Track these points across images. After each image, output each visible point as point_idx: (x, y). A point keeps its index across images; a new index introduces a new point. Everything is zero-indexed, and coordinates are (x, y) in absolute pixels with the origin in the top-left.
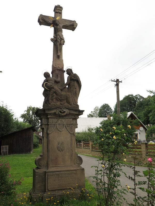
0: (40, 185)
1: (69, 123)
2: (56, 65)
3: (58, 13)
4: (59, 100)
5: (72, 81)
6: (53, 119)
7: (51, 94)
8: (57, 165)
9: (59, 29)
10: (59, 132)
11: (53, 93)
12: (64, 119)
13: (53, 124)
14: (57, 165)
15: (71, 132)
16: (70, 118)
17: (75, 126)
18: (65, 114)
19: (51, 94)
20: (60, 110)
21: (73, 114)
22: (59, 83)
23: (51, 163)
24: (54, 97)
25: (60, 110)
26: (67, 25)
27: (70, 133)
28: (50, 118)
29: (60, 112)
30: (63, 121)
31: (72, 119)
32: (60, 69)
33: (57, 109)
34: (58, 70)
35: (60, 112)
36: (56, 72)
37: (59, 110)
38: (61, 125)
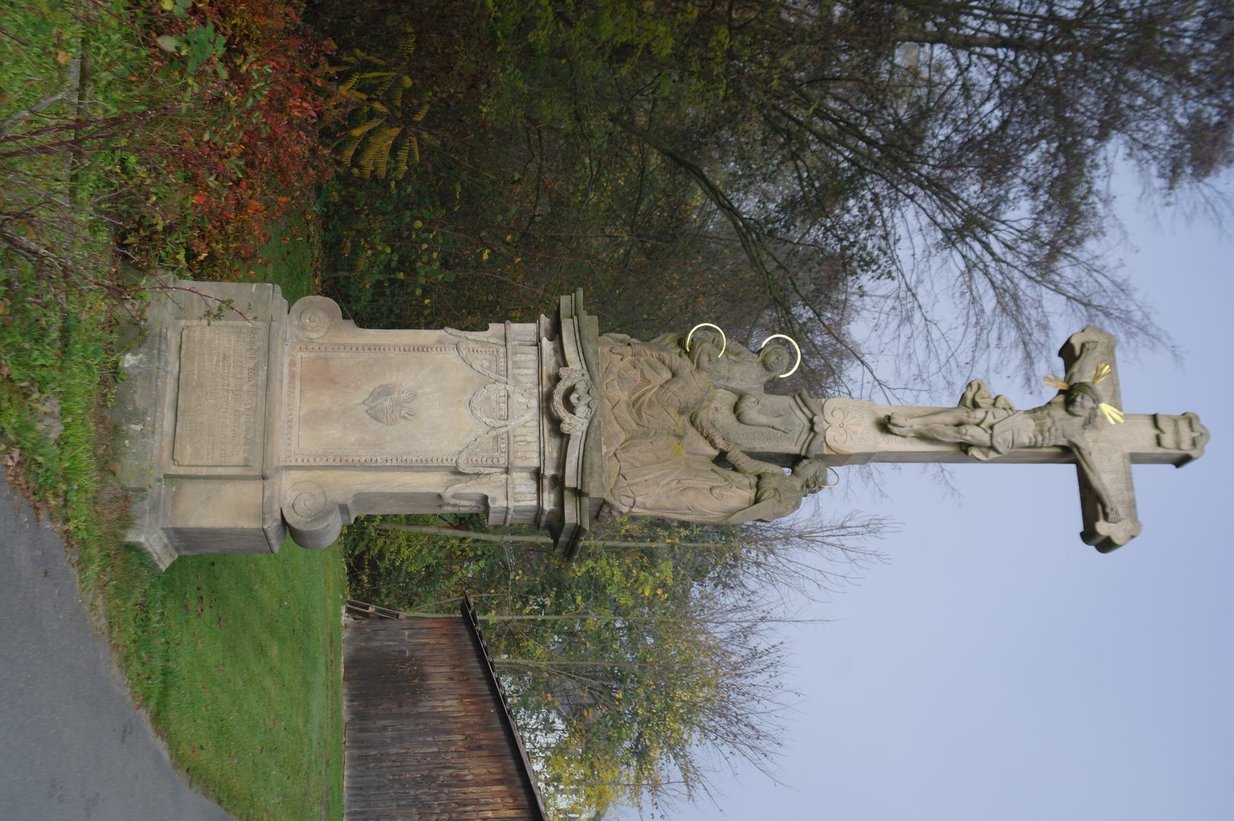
1: (513, 447)
2: (838, 414)
3: (1157, 432)
4: (637, 394)
5: (754, 480)
6: (534, 365)
7: (665, 355)
8: (298, 383)
9: (1049, 414)
10: (466, 398)
12: (536, 423)
13: (510, 366)
15: (465, 454)
16: (541, 453)
17: (503, 491)
18: (561, 412)
19: (665, 355)
20: (578, 386)
21: (561, 465)
22: (733, 418)
23: (313, 355)
24: (649, 374)
25: (581, 387)
26: (1092, 471)
29: (572, 389)
30: (528, 417)
31: (535, 463)
32: (816, 429)
33: (585, 371)
34: (811, 421)
35: (572, 389)
36: (798, 412)
37: (583, 383)
38: (504, 406)
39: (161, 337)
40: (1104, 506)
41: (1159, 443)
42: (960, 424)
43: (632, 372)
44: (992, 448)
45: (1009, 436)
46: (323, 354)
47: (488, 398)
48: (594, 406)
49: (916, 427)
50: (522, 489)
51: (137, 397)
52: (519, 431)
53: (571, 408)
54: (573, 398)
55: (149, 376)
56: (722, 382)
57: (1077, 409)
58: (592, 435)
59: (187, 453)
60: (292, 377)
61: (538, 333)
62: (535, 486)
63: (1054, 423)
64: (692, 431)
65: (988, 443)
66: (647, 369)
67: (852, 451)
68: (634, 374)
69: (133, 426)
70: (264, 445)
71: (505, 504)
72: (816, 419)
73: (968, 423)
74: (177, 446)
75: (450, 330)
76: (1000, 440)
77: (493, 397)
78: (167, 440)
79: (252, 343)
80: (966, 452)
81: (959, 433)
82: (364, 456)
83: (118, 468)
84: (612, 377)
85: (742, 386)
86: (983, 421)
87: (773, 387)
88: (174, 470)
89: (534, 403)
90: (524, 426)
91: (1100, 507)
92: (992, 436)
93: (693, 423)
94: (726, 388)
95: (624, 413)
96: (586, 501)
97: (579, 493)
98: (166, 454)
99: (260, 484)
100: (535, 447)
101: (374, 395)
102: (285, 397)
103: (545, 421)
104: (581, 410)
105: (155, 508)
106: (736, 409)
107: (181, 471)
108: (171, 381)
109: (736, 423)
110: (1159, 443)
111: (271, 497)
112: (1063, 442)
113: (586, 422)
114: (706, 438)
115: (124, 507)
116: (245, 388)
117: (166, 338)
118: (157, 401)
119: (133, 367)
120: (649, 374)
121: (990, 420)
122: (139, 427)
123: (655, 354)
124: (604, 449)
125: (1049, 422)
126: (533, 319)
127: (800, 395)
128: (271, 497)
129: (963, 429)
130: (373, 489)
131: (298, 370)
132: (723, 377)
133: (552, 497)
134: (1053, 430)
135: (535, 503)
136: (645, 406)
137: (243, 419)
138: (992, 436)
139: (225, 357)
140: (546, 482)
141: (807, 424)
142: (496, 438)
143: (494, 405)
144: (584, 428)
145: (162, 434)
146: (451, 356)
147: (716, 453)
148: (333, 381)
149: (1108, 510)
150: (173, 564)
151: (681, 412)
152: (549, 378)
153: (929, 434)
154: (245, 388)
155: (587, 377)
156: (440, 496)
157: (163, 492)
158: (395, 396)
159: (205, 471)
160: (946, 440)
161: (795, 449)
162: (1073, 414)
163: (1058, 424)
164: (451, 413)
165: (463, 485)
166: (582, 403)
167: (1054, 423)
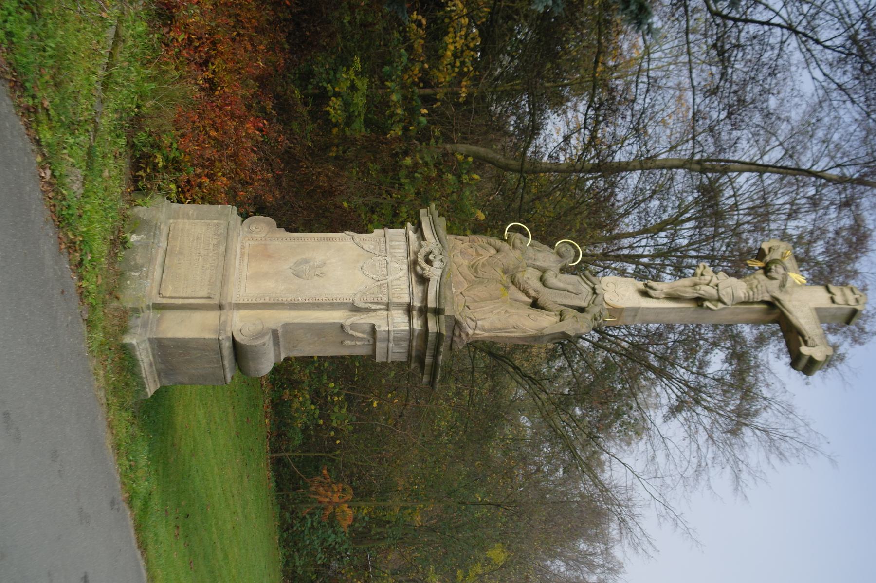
3: (830, 295)
8: (246, 259)
11: (495, 248)
12: (406, 278)
14: (246, 259)
16: (411, 294)
17: (385, 321)
21: (425, 298)
24: (481, 251)
25: (436, 252)
26: (791, 313)
29: (430, 252)
31: (406, 299)
32: (597, 292)
34: (594, 289)
39: (157, 227)
40: (803, 337)
41: (833, 301)
42: (696, 284)
43: (470, 250)
44: (720, 300)
45: (729, 290)
49: (665, 290)
50: (399, 320)
51: (138, 258)
52: (395, 283)
53: (429, 262)
54: (431, 257)
55: (146, 246)
56: (530, 261)
57: (773, 274)
58: (445, 276)
59: (169, 291)
60: (243, 255)
62: (407, 319)
63: (759, 282)
64: (512, 287)
65: (716, 296)
66: (479, 249)
67: (623, 306)
68: (472, 251)
69: (133, 273)
70: (222, 287)
71: (387, 329)
72: (596, 286)
73: (700, 284)
74: (163, 286)
75: (347, 232)
76: (724, 293)
77: (377, 264)
78: (156, 284)
79: (216, 231)
80: (702, 306)
81: (696, 289)
82: (290, 298)
83: (121, 297)
84: (456, 251)
85: (544, 265)
86: (710, 282)
87: (564, 270)
88: (159, 300)
89: (405, 267)
90: (398, 279)
91: (800, 338)
92: (718, 290)
93: (513, 282)
94: (534, 267)
96: (442, 317)
97: (438, 312)
99: (218, 313)
101: (297, 264)
102: (237, 265)
103: (413, 276)
104: (437, 264)
105: (145, 325)
106: (542, 279)
107: (164, 301)
108: (161, 252)
109: (542, 287)
110: (833, 301)
111: (225, 322)
112: (767, 298)
113: (440, 271)
114: (522, 291)
115: (123, 321)
116: (210, 255)
117: (159, 228)
118: (151, 261)
119: (137, 241)
120: (481, 251)
121: (715, 281)
122: (137, 274)
124: (454, 290)
125: (755, 282)
127: (584, 274)
128: (225, 322)
129: (698, 287)
130: (296, 321)
131: (246, 251)
132: (531, 259)
133: (419, 322)
134: (759, 286)
135: (407, 328)
136: (479, 267)
137: (208, 271)
138: (718, 290)
139: (198, 238)
140: (415, 313)
141: (591, 290)
142: (380, 286)
143: (378, 268)
144: (439, 274)
145: (153, 280)
146: (349, 243)
147: (531, 301)
148: (269, 257)
149: (807, 338)
150: (156, 392)
151: (505, 272)
153: (675, 294)
154: (210, 255)
155: (440, 245)
156: (342, 326)
157: (151, 317)
158: (312, 263)
159: (180, 301)
160: (687, 295)
161: (583, 304)
162: (772, 279)
163: (762, 283)
164: (351, 282)
165: (358, 317)
166: (437, 259)
167: (759, 282)
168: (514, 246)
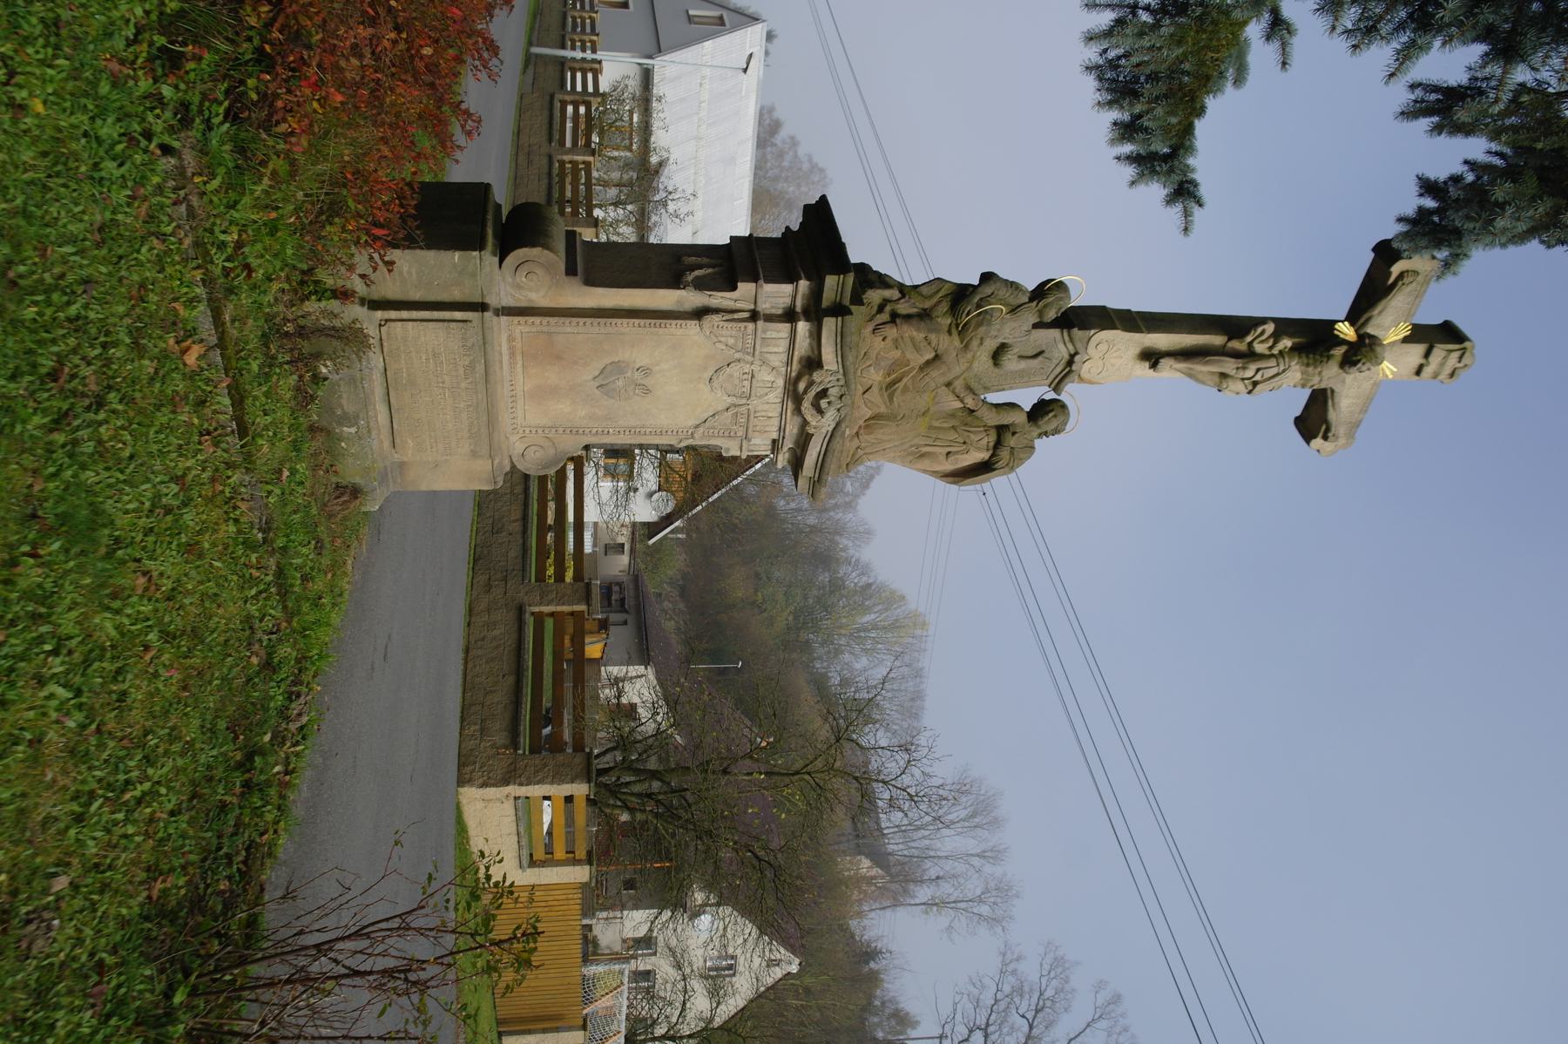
0: (409, 273)
2: (1103, 347)
5: (993, 438)
7: (933, 337)
8: (519, 358)
14: (519, 358)
15: (701, 430)
22: (991, 362)
25: (833, 392)
27: (697, 426)
28: (793, 333)
29: (823, 394)
31: (775, 436)
34: (1072, 356)
35: (823, 394)
36: (1061, 346)
38: (747, 383)
40: (1328, 430)
46: (545, 329)
47: (731, 376)
48: (843, 412)
51: (344, 402)
53: (820, 411)
54: (823, 403)
60: (512, 354)
61: (794, 298)
70: (490, 435)
77: (736, 374)
78: (385, 431)
89: (780, 382)
95: (875, 396)
98: (387, 444)
100: (776, 422)
108: (377, 377)
116: (463, 385)
118: (366, 403)
121: (1258, 377)
122: (353, 430)
123: (922, 335)
126: (791, 279)
137: (464, 415)
141: (1067, 357)
148: (559, 358)
152: (800, 361)
154: (463, 385)
168: (966, 346)
